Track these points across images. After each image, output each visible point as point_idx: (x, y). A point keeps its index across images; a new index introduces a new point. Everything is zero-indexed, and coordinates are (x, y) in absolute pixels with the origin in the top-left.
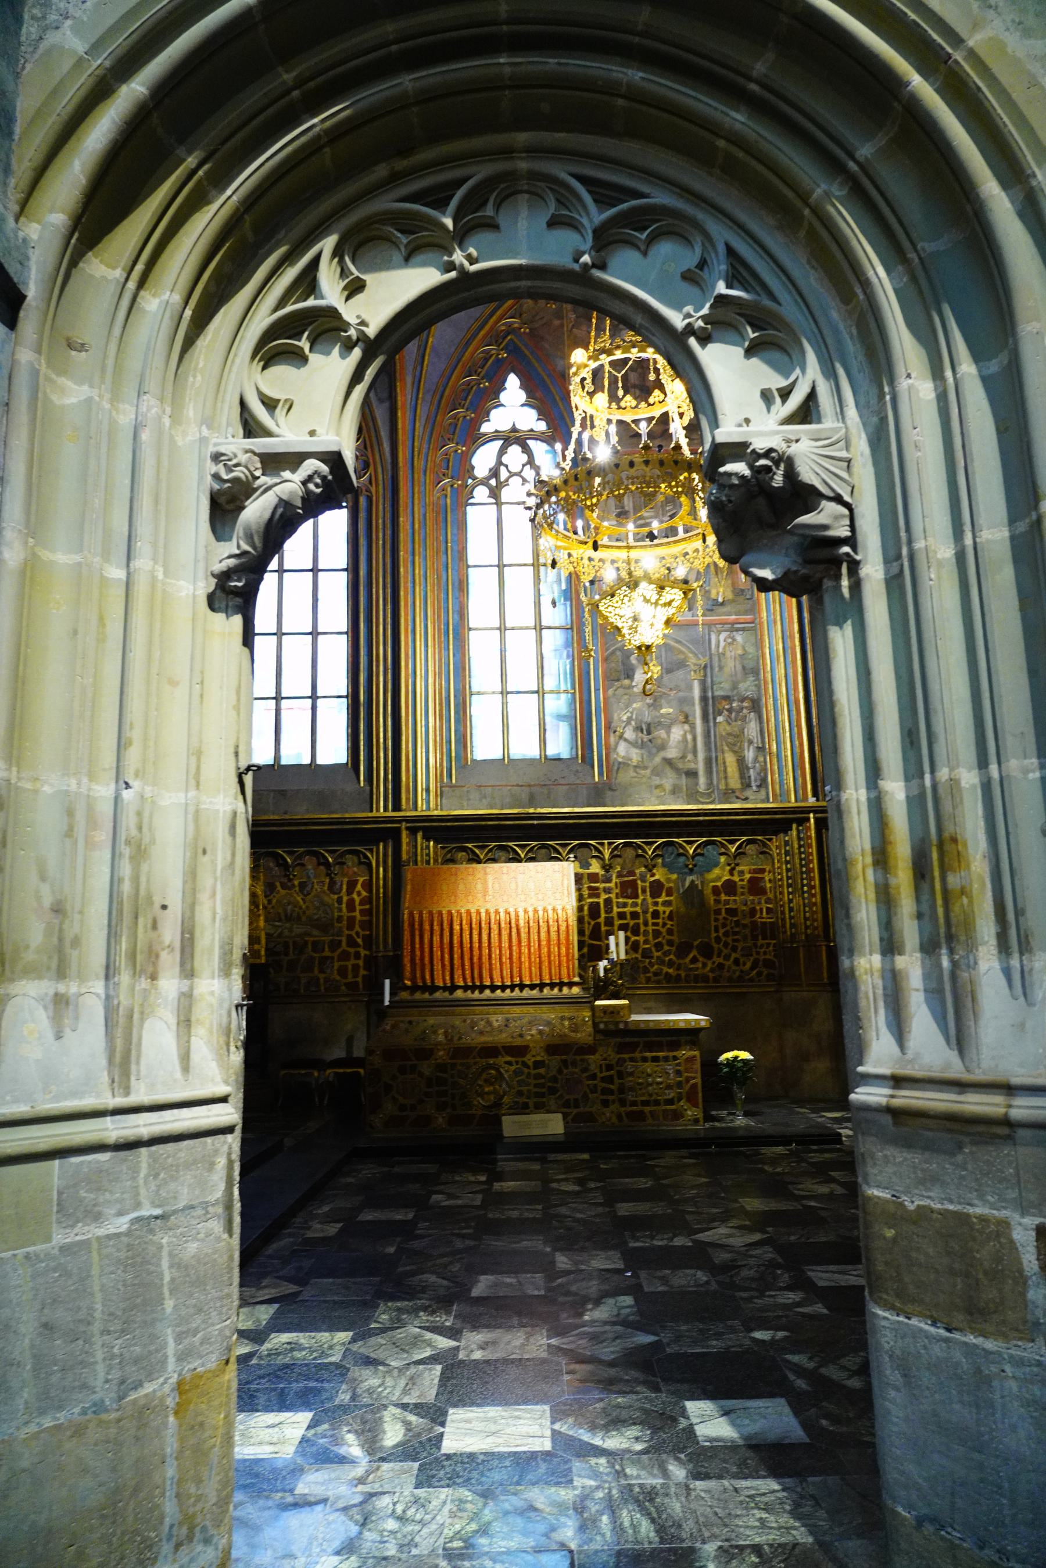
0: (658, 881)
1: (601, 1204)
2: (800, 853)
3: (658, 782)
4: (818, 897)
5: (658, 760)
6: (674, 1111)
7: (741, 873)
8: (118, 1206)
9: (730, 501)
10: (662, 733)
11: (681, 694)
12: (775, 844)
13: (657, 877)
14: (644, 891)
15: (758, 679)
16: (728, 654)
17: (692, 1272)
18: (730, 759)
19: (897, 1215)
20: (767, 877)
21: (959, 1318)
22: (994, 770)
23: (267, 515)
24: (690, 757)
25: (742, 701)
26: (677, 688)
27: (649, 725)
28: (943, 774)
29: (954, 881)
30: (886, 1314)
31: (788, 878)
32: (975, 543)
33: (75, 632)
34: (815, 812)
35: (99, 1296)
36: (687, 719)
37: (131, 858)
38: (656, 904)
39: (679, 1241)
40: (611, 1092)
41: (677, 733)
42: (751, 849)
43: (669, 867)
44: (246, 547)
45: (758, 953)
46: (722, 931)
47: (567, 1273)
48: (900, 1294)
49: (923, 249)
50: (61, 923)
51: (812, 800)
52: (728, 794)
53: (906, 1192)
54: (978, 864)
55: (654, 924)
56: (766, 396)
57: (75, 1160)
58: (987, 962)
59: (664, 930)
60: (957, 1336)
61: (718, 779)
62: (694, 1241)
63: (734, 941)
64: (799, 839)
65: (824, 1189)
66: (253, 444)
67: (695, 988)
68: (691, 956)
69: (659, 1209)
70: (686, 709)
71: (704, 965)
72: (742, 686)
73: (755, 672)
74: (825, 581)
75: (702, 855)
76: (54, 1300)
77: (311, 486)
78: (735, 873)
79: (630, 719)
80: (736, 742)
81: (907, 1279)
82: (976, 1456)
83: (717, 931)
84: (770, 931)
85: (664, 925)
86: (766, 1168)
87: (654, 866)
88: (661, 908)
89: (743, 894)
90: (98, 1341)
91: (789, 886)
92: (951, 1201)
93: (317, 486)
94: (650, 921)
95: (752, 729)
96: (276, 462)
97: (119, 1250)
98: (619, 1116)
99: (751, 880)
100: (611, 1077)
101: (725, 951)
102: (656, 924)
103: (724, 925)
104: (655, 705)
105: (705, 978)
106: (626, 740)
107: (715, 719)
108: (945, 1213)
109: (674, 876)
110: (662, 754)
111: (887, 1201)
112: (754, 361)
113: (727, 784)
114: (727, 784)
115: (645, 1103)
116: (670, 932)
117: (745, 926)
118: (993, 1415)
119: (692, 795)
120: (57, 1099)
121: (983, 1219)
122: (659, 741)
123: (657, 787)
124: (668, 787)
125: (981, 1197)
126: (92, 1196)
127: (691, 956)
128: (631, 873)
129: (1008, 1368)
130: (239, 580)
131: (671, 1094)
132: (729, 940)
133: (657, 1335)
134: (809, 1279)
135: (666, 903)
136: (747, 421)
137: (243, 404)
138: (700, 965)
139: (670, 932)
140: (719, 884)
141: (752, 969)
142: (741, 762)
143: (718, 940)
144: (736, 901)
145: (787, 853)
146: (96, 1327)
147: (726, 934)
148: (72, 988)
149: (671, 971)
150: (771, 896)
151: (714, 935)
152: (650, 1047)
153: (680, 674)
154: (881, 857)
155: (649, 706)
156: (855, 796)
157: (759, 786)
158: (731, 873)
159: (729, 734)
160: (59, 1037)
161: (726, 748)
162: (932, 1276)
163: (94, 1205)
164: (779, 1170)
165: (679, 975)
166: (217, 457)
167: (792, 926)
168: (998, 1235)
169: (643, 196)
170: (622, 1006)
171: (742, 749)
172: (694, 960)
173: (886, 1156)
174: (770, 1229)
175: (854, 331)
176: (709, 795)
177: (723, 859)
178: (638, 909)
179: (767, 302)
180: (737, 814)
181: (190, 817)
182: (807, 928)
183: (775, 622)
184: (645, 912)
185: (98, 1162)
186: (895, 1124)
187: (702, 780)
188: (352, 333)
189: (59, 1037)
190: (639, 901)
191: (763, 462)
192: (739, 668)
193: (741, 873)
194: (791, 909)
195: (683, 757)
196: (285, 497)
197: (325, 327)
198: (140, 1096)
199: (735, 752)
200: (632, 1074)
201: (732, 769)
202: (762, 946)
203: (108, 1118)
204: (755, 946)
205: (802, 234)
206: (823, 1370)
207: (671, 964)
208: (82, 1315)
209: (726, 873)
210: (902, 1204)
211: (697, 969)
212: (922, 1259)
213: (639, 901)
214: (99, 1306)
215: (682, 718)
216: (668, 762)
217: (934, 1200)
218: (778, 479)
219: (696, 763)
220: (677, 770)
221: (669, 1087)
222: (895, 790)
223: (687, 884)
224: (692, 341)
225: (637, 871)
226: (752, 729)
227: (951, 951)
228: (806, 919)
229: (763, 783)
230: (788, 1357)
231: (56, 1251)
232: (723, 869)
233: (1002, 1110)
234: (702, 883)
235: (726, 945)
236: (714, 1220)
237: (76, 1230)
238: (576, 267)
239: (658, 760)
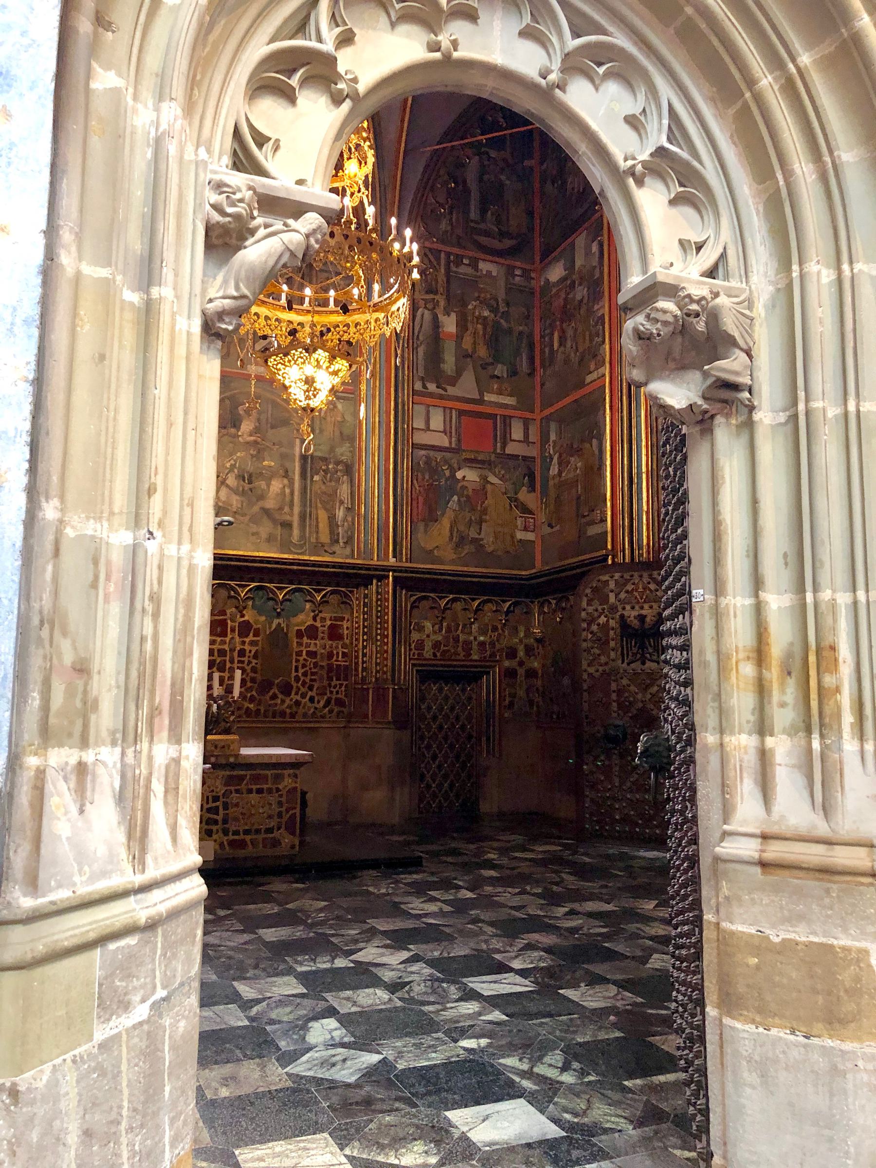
1: (243, 932)
2: (377, 606)
4: (390, 645)
5: (256, 509)
6: (274, 838)
7: (323, 619)
8: (142, 992)
9: (659, 335)
10: (263, 484)
11: (283, 450)
12: (357, 596)
13: (246, 618)
14: (233, 630)
15: (353, 446)
16: (329, 419)
17: (371, 990)
18: (323, 515)
19: (760, 946)
20: (345, 624)
21: (819, 1027)
22: (861, 595)
23: (271, 263)
24: (287, 509)
26: (280, 444)
28: (826, 595)
29: (829, 680)
30: (747, 1027)
31: (364, 627)
32: (858, 411)
33: (102, 357)
34: (394, 571)
35: (126, 1092)
36: (286, 474)
37: (153, 615)
38: (244, 643)
39: (341, 963)
40: (216, 822)
41: (276, 485)
42: (334, 599)
44: (246, 292)
45: (331, 692)
46: (301, 671)
47: (258, 1001)
48: (760, 1011)
49: (839, 157)
50: (86, 685)
51: (392, 560)
52: (318, 547)
53: (773, 926)
54: (846, 670)
55: (239, 662)
56: (683, 244)
57: (112, 946)
58: (850, 745)
60: (815, 1041)
61: (310, 532)
62: (352, 961)
63: (311, 680)
64: (378, 593)
65: (432, 908)
66: (252, 180)
67: (264, 722)
69: (299, 932)
70: (288, 465)
71: (283, 701)
72: (339, 451)
73: (351, 439)
74: (718, 416)
75: (290, 600)
76: (94, 1104)
77: (312, 241)
78: (318, 619)
79: (233, 466)
80: (330, 500)
81: (768, 997)
82: (827, 1132)
83: (297, 670)
84: (343, 673)
85: (249, 662)
86: (371, 889)
87: (245, 608)
89: (323, 638)
90: (124, 1140)
91: (364, 634)
92: (815, 933)
93: (317, 241)
95: (344, 490)
96: (271, 204)
97: (141, 1041)
98: (221, 845)
99: (332, 627)
100: (217, 807)
101: (303, 690)
102: (243, 662)
103: (304, 666)
104: (259, 456)
105: (283, 714)
106: (228, 486)
107: (312, 477)
108: (809, 945)
109: (263, 618)
110: (260, 504)
111: (752, 936)
112: (675, 211)
114: (317, 539)
115: (247, 832)
116: (254, 670)
117: (322, 667)
118: (846, 1099)
119: (285, 546)
120: (92, 879)
121: (844, 949)
122: (260, 492)
123: (253, 534)
124: (264, 535)
125: (845, 930)
126: (124, 984)
128: (224, 613)
129: (860, 1063)
130: (230, 323)
131: (273, 823)
133: (379, 1053)
134: (472, 989)
135: (252, 643)
136: (672, 265)
137: (237, 133)
139: (254, 670)
140: (303, 628)
141: (325, 707)
142: (332, 518)
143: (297, 679)
144: (315, 645)
145: (365, 605)
146: (124, 1125)
147: (305, 674)
148: (89, 756)
149: (251, 706)
150: (347, 642)
151: (294, 674)
152: (256, 779)
153: (284, 430)
154: (760, 655)
156: (733, 601)
158: (314, 619)
159: (325, 493)
160: (82, 811)
161: (319, 505)
162: (794, 995)
163: (126, 994)
164: (383, 891)
165: (259, 710)
166: (219, 186)
167: (364, 669)
168: (858, 960)
169: (605, 33)
170: (233, 741)
173: (753, 899)
174: (411, 947)
175: (761, 209)
176: (301, 546)
177: (308, 605)
178: (226, 647)
179: (695, 164)
180: (327, 566)
181: (184, 572)
182: (377, 672)
183: (374, 397)
184: (232, 650)
185: (129, 946)
186: (763, 873)
187: (296, 532)
188: (341, 86)
189: (82, 811)
190: (228, 639)
191: (694, 307)
192: (337, 433)
193: (323, 619)
194: (364, 655)
195: (281, 509)
196: (292, 247)
197: (321, 71)
198: (152, 873)
199: (326, 509)
200: (237, 805)
201: (323, 525)
202: (335, 687)
203: (132, 898)
205: (731, 111)
206: (536, 1070)
207: (252, 700)
208: (114, 1115)
209: (310, 618)
210: (767, 938)
212: (785, 981)
213: (228, 639)
214: (125, 1104)
216: (266, 512)
217: (801, 935)
218: (701, 326)
219: (291, 514)
220: (274, 521)
221: (270, 817)
222: (777, 601)
223: (274, 626)
224: (631, 181)
225: (228, 612)
226: (344, 490)
227: (822, 736)
228: (377, 664)
229: (349, 541)
230: (501, 1061)
231: (96, 1050)
232: (308, 616)
233: (870, 864)
234: (287, 626)
236: (356, 941)
237: (112, 1024)
238: (543, 82)
239: (256, 509)
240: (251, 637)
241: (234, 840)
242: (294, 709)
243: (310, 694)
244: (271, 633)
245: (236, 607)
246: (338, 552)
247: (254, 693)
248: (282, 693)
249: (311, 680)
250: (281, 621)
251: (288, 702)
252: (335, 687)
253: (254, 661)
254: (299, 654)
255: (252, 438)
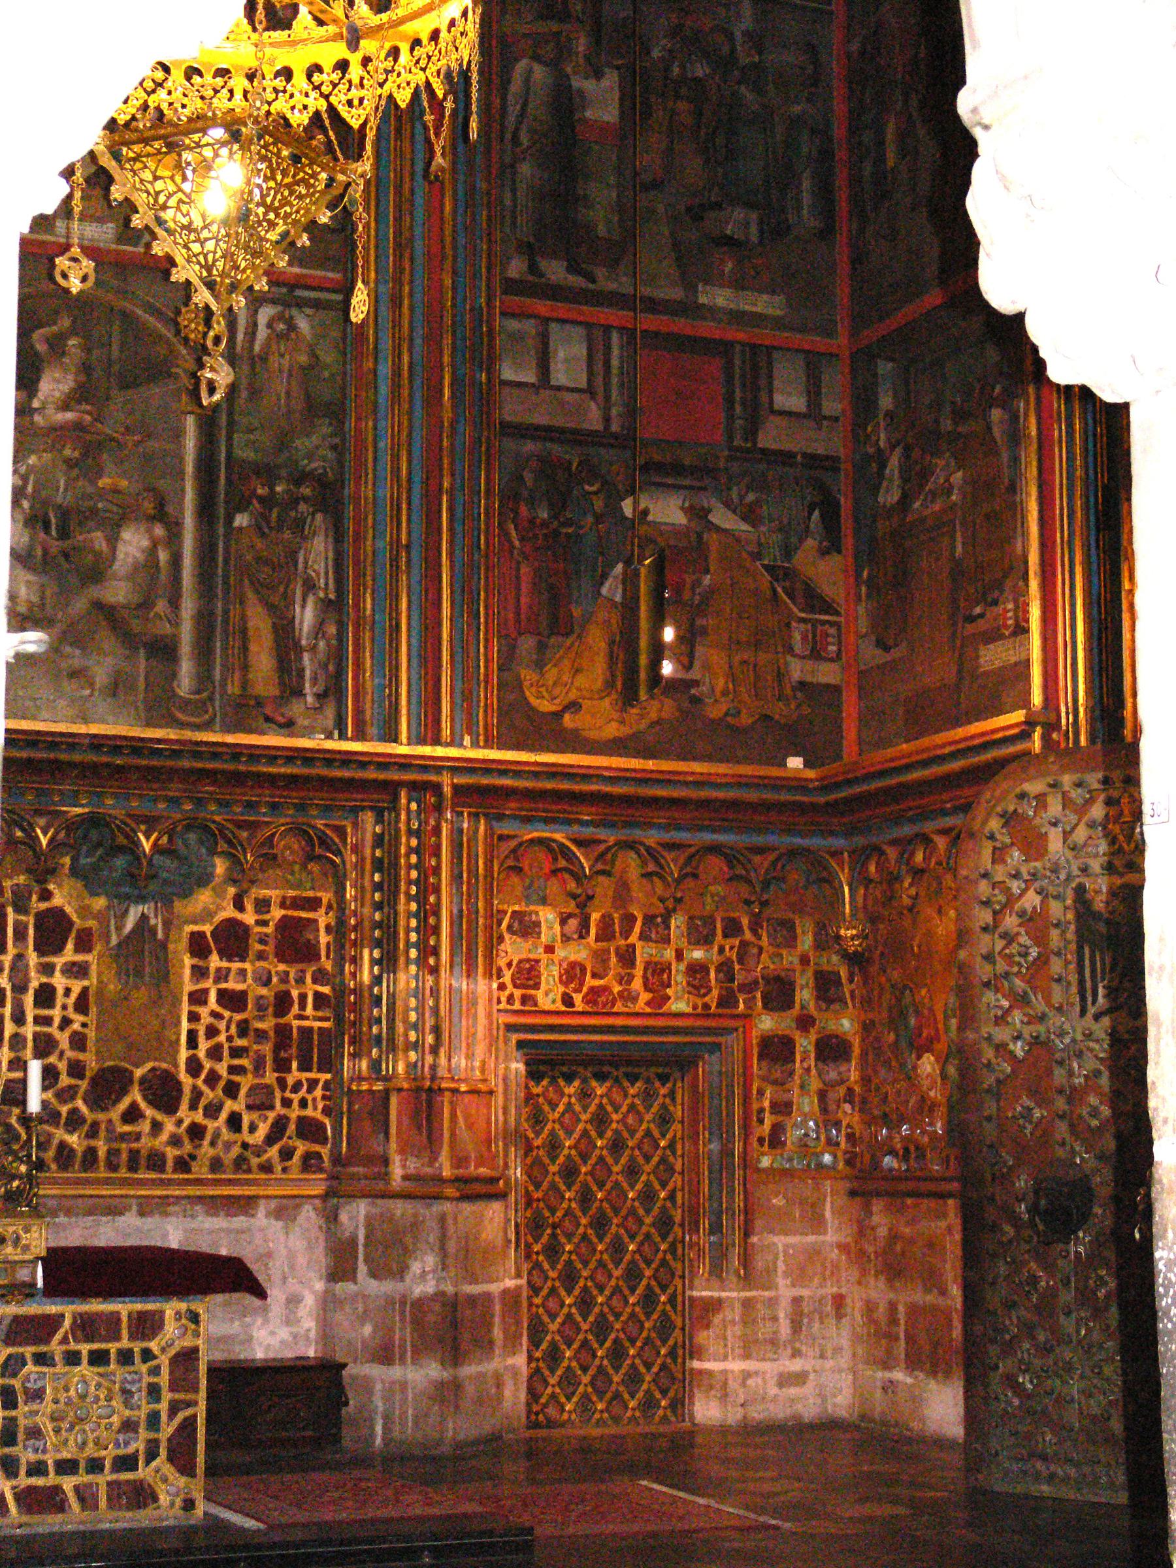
0: (59, 913)
3: (76, 663)
13: (57, 901)
14: (20, 935)
20: (323, 919)
24: (161, 606)
25: (298, 482)
27: (65, 514)
41: (133, 543)
43: (89, 879)
45: (287, 1103)
59: (63, 1038)
68: (124, 1105)
71: (157, 1127)
78: (249, 906)
83: (192, 1042)
85: (66, 1022)
87: (52, 871)
88: (59, 981)
89: (261, 956)
94: (30, 1013)
101: (209, 1095)
102: (48, 1021)
103: (212, 1032)
105: (156, 1161)
107: (229, 519)
109: (100, 903)
113: (245, 684)
114: (245, 684)
115: (66, 1467)
116: (78, 1042)
117: (261, 1035)
123: (74, 674)
124: (101, 675)
127: (124, 1105)
132: (222, 1069)
135: (77, 970)
138: (146, 1127)
140: (207, 928)
141: (270, 1140)
147: (215, 1053)
149: (73, 1139)
150: (328, 966)
151: (184, 1054)
155: (70, 463)
157: (321, 697)
165: (91, 1152)
171: (289, 599)
172: (132, 1115)
176: (202, 706)
184: (20, 988)
193: (263, 905)
195: (146, 605)
202: (296, 1087)
204: (282, 1083)
207: (74, 1121)
211: (138, 1137)
215: (149, 506)
219: (176, 623)
223: (130, 923)
232: (219, 893)
234: (167, 924)
235: (212, 1079)
239: (80, 605)
240: (69, 954)
241: (31, 1489)
242: (188, 1147)
243: (229, 1106)
244: (124, 943)
245: (29, 871)
246: (303, 722)
247: (80, 1103)
248: (152, 1103)
249: (232, 1070)
250: (146, 908)
251: (169, 1127)
252: (296, 1087)
253: (78, 1019)
254: (198, 998)
255: (69, 416)
